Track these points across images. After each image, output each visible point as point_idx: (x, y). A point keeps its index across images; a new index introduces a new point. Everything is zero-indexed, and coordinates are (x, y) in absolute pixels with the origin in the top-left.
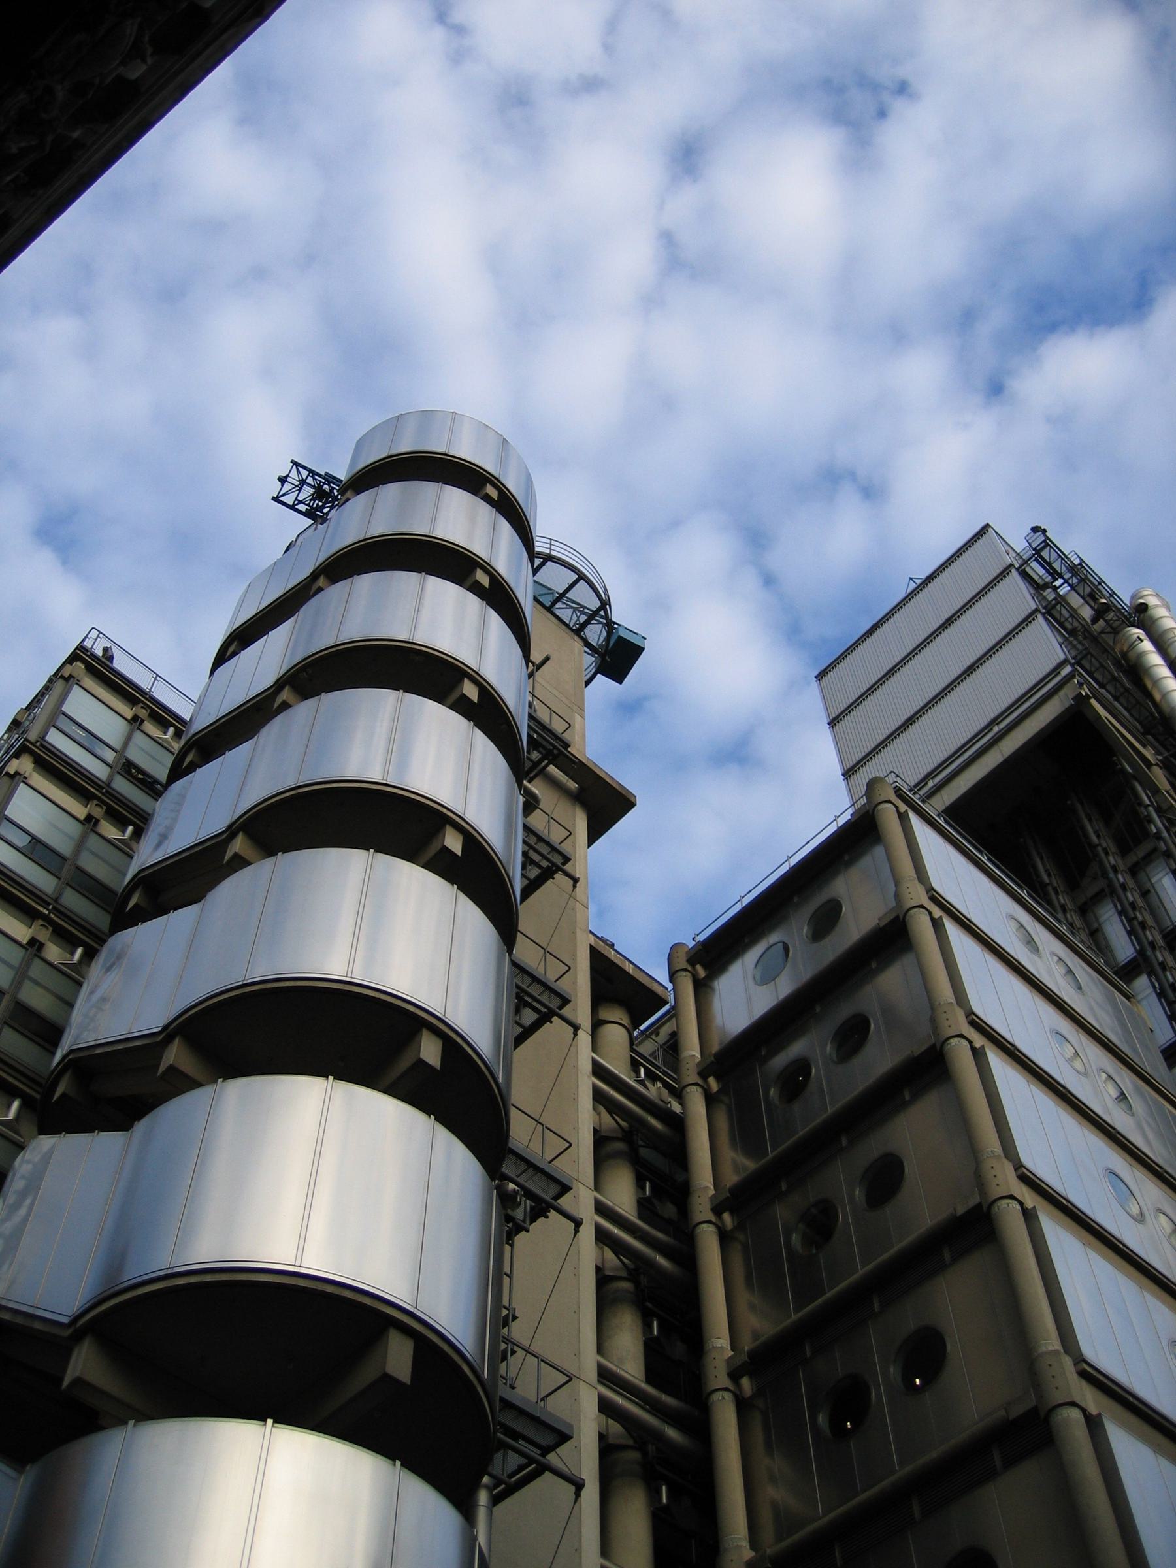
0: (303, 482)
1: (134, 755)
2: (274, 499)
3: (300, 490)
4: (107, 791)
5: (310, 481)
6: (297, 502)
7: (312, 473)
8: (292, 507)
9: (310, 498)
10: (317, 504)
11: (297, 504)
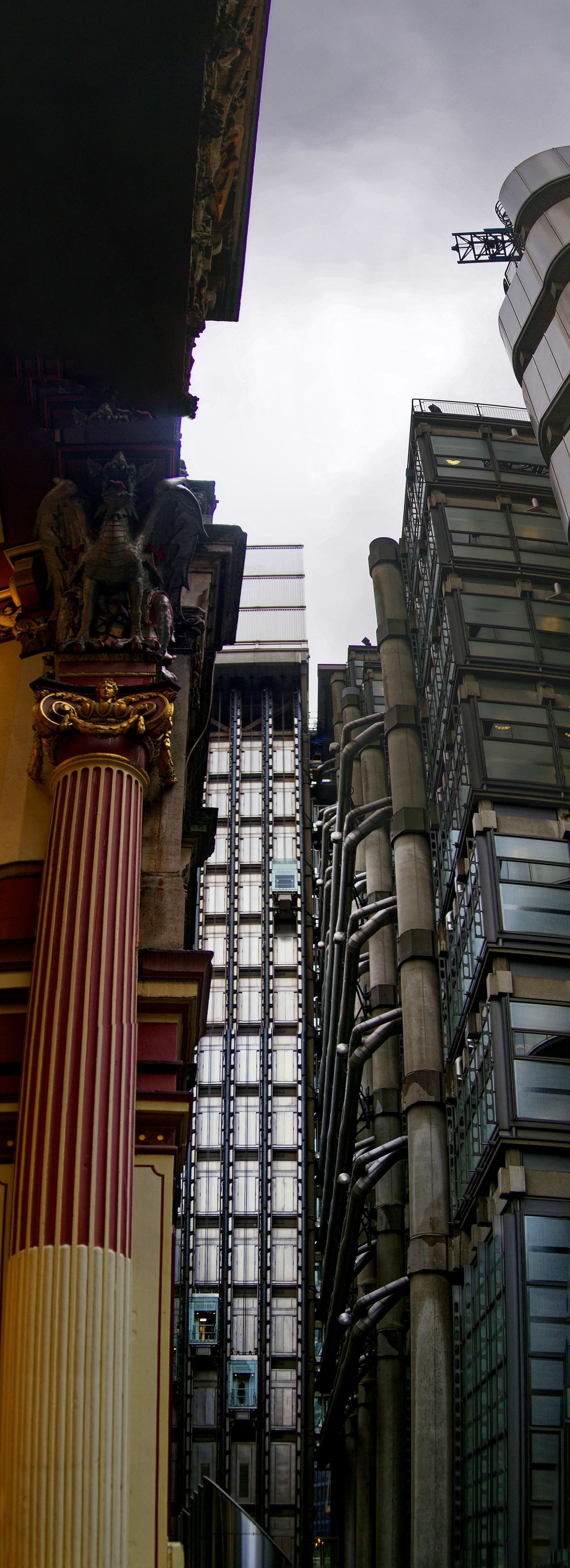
1: (500, 456)
4: (502, 486)
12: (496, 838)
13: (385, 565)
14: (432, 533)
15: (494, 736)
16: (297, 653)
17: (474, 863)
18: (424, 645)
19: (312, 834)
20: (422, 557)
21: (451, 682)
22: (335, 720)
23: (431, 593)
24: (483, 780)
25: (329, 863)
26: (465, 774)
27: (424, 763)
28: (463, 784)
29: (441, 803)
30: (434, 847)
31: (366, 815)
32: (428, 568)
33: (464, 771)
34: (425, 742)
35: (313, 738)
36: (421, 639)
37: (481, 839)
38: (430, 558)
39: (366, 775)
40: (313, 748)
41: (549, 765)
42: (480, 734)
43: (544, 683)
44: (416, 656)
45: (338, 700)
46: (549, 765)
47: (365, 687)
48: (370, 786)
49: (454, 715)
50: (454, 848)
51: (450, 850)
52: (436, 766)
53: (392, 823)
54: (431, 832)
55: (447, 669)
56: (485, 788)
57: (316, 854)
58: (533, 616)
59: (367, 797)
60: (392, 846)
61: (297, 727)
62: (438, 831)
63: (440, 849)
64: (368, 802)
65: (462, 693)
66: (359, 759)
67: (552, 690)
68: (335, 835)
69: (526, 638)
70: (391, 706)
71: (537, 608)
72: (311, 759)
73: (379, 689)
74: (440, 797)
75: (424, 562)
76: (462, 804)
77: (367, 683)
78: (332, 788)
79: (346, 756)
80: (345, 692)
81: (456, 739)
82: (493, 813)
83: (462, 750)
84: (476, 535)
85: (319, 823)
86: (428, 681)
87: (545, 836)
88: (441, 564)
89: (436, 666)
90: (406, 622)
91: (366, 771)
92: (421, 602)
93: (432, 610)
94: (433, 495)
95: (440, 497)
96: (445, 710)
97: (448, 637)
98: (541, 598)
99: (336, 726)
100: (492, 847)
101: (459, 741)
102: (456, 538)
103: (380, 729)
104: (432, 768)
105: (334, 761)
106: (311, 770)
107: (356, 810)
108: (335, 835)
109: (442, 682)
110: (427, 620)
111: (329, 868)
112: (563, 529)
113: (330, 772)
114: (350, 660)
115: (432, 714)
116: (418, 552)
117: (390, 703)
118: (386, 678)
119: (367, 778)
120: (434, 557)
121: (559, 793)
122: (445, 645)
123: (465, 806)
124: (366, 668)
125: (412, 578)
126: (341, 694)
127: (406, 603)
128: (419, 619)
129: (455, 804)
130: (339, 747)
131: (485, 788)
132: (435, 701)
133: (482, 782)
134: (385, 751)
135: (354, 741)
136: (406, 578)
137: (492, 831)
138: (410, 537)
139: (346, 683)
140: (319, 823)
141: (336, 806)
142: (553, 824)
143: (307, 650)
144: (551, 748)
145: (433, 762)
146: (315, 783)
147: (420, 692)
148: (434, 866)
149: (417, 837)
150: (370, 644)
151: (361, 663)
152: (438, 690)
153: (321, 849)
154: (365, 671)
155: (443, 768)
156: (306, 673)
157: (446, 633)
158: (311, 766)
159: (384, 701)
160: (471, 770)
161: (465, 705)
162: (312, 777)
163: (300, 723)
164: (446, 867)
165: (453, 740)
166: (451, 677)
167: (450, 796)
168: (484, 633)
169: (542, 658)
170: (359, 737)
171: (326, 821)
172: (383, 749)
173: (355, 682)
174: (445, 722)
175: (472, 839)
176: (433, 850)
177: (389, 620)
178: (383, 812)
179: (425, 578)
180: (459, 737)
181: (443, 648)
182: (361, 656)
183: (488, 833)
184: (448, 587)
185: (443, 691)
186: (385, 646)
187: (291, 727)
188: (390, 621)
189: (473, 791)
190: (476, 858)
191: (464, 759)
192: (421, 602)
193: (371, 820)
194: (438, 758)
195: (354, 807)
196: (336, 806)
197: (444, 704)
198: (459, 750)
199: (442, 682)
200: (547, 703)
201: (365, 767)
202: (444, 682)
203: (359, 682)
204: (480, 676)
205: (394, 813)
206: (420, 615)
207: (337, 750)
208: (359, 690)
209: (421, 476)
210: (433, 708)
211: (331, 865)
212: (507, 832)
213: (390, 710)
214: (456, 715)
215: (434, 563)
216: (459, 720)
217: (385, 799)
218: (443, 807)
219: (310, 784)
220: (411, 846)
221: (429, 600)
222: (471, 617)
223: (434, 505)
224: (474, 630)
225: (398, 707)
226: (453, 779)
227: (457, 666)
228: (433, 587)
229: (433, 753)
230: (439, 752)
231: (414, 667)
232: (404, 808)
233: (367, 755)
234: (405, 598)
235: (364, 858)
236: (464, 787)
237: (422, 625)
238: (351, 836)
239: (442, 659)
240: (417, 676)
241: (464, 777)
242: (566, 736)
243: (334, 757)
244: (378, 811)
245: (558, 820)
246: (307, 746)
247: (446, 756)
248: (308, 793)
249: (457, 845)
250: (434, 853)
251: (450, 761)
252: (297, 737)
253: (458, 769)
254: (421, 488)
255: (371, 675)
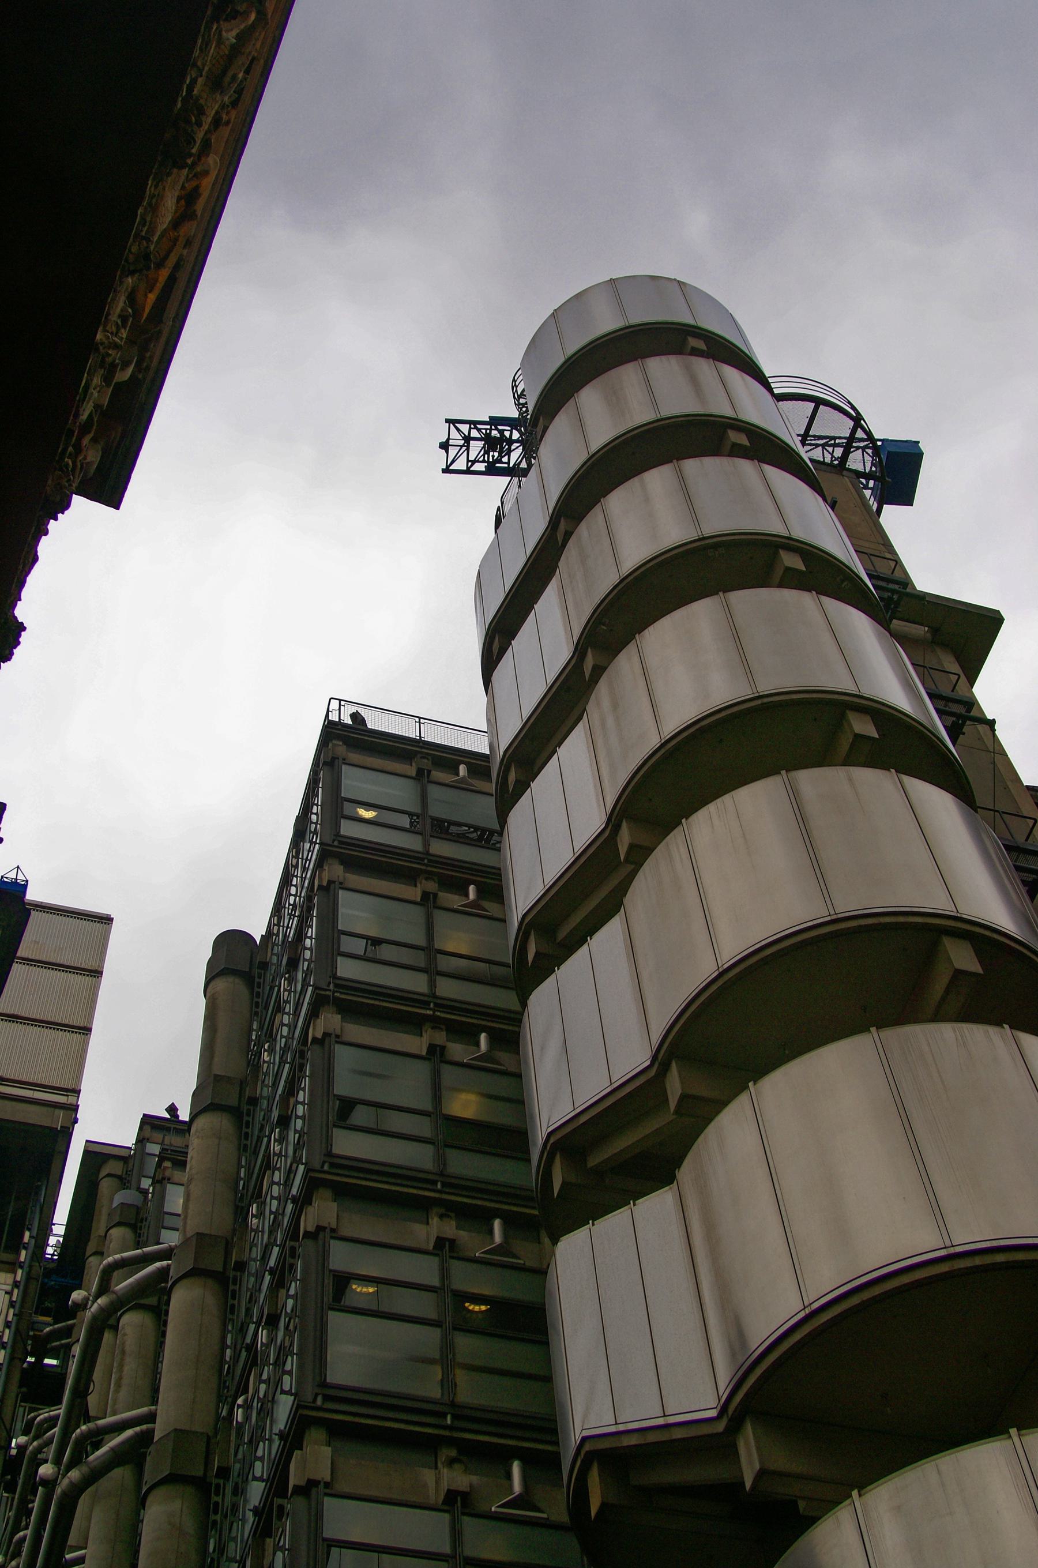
0: (468, 439)
1: (437, 810)
2: (444, 471)
3: (468, 450)
4: (429, 861)
5: (475, 434)
6: (470, 464)
7: (473, 424)
8: (468, 471)
9: (482, 452)
10: (493, 456)
11: (471, 466)
12: (327, 1500)
13: (231, 979)
14: (312, 932)
15: (347, 1303)
16: (57, 1111)
17: (282, 1549)
18: (262, 1128)
19: (5, 1460)
20: (288, 972)
21: (294, 1200)
22: (91, 1248)
23: (290, 1037)
24: (319, 1386)
25: (24, 1523)
26: (290, 1373)
27: (223, 1346)
28: (283, 1392)
29: (240, 1426)
30: (216, 1512)
31: (107, 1437)
32: (295, 992)
33: (288, 1367)
34: (233, 1306)
35: (48, 1273)
36: (260, 1116)
37: (300, 1502)
38: (300, 976)
39: (122, 1359)
40: (45, 1292)
41: (432, 1361)
42: (325, 1299)
43: (442, 1211)
44: (246, 1146)
45: (105, 1212)
46: (432, 1361)
47: (153, 1193)
48: (125, 1381)
49: (289, 1260)
50: (250, 1517)
51: (244, 1520)
52: (244, 1354)
53: (148, 1458)
54: (214, 1481)
55: (292, 1176)
56: (319, 1401)
57: (4, 1501)
58: (440, 1089)
59: (115, 1401)
60: (142, 1502)
61: (25, 1248)
62: (228, 1480)
63: (226, 1517)
64: (114, 1413)
65: (308, 1223)
66: (115, 1328)
67: (453, 1223)
68: (46, 1470)
69: (423, 1127)
70: (189, 1235)
71: (449, 1074)
72: (36, 1313)
73: (175, 1200)
74: (239, 1415)
75: (291, 980)
76: (276, 1430)
77: (158, 1186)
78: (58, 1377)
79: (95, 1318)
80: (121, 1197)
81: (285, 1304)
82: (327, 1451)
83: (291, 1327)
84: (376, 942)
85: (22, 1439)
86: (258, 1195)
87: (413, 1499)
88: (316, 988)
89: (275, 1169)
90: (242, 1084)
91: (123, 1352)
92: (271, 1051)
93: (287, 1066)
94: (326, 867)
95: (335, 870)
96: (276, 1249)
97: (303, 1118)
98: (457, 1058)
99: (91, 1259)
100: (317, 1518)
101: (289, 1310)
102: (349, 945)
103: (164, 1273)
104: (236, 1358)
105: (73, 1325)
106: (31, 1333)
107: (91, 1425)
108: (46, 1470)
109: (278, 1199)
110: (275, 1085)
111: (21, 1534)
112: (507, 939)
113: (62, 1345)
114: (141, 1140)
115: (254, 1255)
116: (284, 962)
117: (188, 1228)
118: (190, 1180)
119: (121, 1366)
120: (307, 973)
121: (444, 1415)
122: (296, 1131)
123: (282, 1435)
124: (162, 1158)
125: (266, 1008)
126: (112, 1200)
127: (248, 1050)
128: (263, 1082)
129: (264, 1429)
130: (86, 1299)
131: (319, 1401)
132: (263, 1231)
133: (317, 1390)
134: (163, 1318)
135: (114, 1292)
136: (257, 1003)
137: (321, 1486)
138: (278, 935)
139: (124, 1181)
140: (22, 1439)
141: (61, 1411)
142: (428, 1476)
143: (76, 1108)
144: (439, 1330)
145: (239, 1347)
146: (33, 1360)
147: (241, 1213)
148: (211, 1550)
149: (190, 1490)
150: (178, 1116)
151: (154, 1149)
152: (271, 1212)
153: (15, 1493)
154: (159, 1164)
155: (254, 1360)
156: (63, 1149)
157: (300, 1110)
158: (32, 1325)
159: (178, 1223)
160: (301, 1367)
161: (309, 1243)
162: (29, 1348)
163: (33, 1241)
164: (231, 1554)
165: (280, 1306)
166: (294, 1191)
167: (258, 1414)
168: (360, 1116)
169: (445, 1165)
170: (123, 1285)
171: (36, 1437)
172: (160, 1314)
173: (139, 1181)
174: (272, 1272)
175: (283, 1501)
176: (213, 1517)
177: (216, 1076)
178: (137, 1434)
179: (287, 1010)
180: (290, 1302)
181: (293, 1137)
182: (158, 1136)
183: (314, 1490)
184: (317, 1030)
185: (278, 1214)
186: (201, 1122)
187: (16, 1245)
188: (218, 1078)
189: (299, 1405)
190: (286, 1541)
191: (292, 1344)
192: (271, 1051)
193: (112, 1449)
194: (248, 1340)
195: (88, 1419)
196: (61, 1411)
197: (276, 1240)
198: (287, 1328)
199: (278, 1199)
200: (444, 1247)
201: (123, 1344)
202: (282, 1200)
203: (146, 1183)
204: (342, 1192)
205: (156, 1439)
206: (267, 1074)
207: (83, 1306)
208: (141, 1197)
209: (315, 832)
210: (256, 1245)
211: (27, 1528)
212: (347, 1489)
213: (186, 1242)
214: (292, 1261)
215: (305, 985)
216: (296, 1271)
217: (144, 1410)
218: (243, 1434)
219: (25, 1361)
220: (177, 1505)
221: (285, 1050)
222: (344, 1086)
223: (325, 883)
224: (347, 1106)
225: (200, 1236)
226: (267, 1382)
227: (308, 1170)
228: (295, 1027)
229: (243, 1330)
230: (252, 1327)
231: (239, 1166)
232: (176, 1430)
233: (130, 1321)
234: (250, 1040)
235: (89, 1519)
236: (284, 1397)
237: (265, 1092)
238: (74, 1474)
239: (286, 1156)
240: (242, 1183)
241: (286, 1378)
242: (467, 1309)
243: (74, 1318)
244: (129, 1433)
245: (436, 1468)
246: (34, 1288)
247: (263, 1335)
248: (16, 1377)
249: (256, 1511)
250: (215, 1522)
251: (267, 1346)
252: (21, 1267)
253: (279, 1362)
254: (312, 852)
255: (167, 1173)
